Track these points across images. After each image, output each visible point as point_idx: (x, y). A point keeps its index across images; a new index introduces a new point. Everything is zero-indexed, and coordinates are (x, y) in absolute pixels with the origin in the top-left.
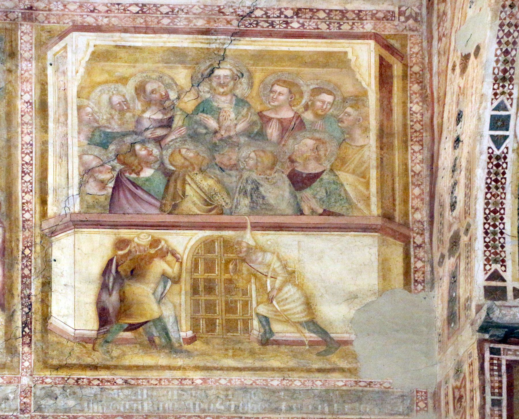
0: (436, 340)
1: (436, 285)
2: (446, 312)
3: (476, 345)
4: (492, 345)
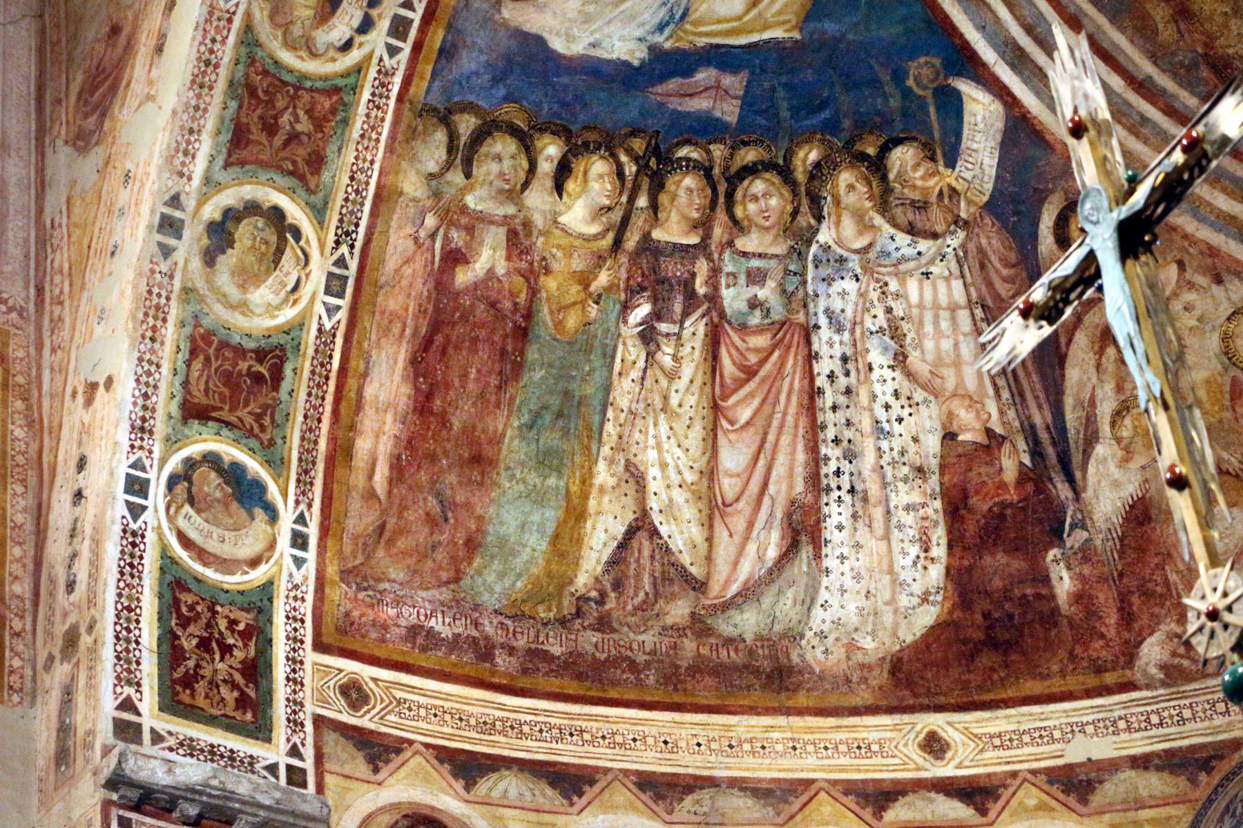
0: (36, 787)
1: (39, 700)
2: (53, 746)
3: (98, 808)
4: (121, 812)
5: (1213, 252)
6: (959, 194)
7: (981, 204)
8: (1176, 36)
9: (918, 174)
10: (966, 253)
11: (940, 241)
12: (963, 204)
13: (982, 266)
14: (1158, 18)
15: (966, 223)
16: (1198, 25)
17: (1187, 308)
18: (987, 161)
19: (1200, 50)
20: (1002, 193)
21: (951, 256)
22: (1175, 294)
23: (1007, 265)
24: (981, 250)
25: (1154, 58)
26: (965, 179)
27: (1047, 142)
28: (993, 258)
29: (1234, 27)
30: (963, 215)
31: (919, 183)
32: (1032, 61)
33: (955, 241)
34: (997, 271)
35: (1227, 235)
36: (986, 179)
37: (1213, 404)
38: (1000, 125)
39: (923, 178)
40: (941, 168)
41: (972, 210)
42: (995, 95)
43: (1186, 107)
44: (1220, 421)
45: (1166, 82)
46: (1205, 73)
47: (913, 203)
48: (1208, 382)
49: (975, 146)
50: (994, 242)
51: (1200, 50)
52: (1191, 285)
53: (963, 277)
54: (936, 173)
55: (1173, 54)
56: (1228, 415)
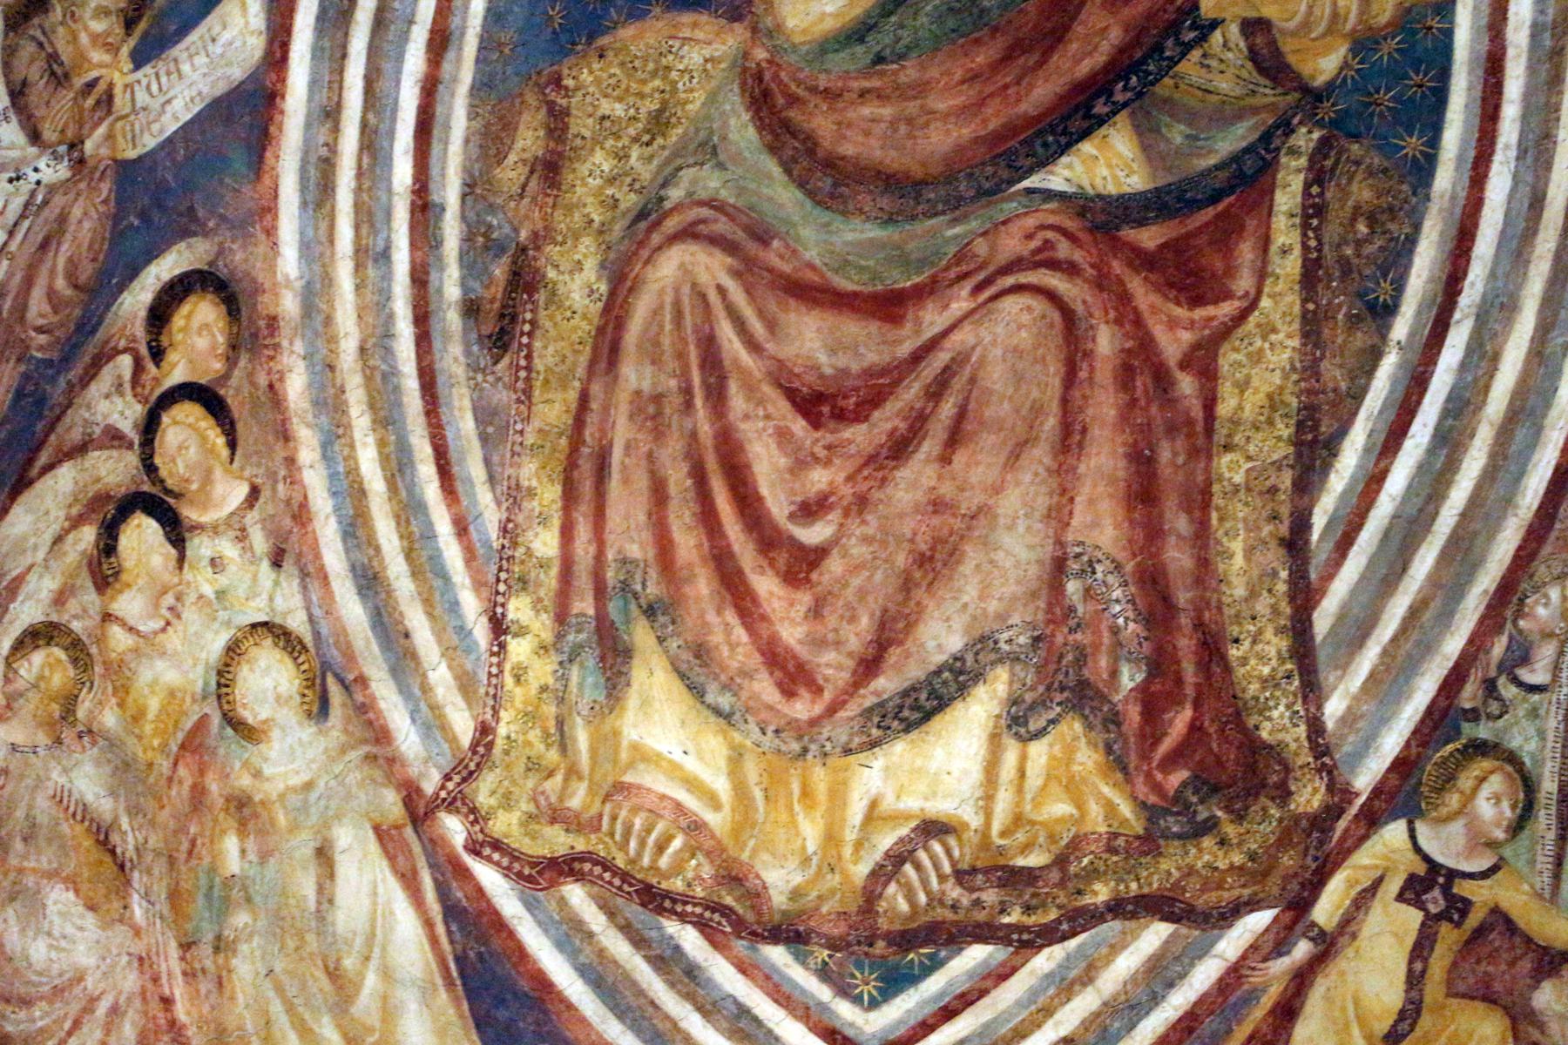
5: (301, 514)
6: (109, 112)
7: (119, 157)
8: (516, 189)
9: (98, 26)
10: (46, 202)
11: (33, 150)
12: (101, 130)
13: (44, 246)
14: (519, 144)
15: (81, 161)
16: (550, 201)
17: (216, 563)
18: (178, 104)
19: (523, 235)
20: (152, 170)
21: (25, 187)
22: (215, 530)
23: (71, 276)
24: (62, 219)
25: (469, 189)
26: (133, 100)
27: (261, 158)
28: (65, 247)
29: (582, 248)
30: (89, 146)
31: (84, 39)
32: (346, 34)
33: (51, 171)
34: (53, 272)
35: (337, 509)
36: (155, 127)
37: (156, 732)
38: (237, 74)
39: (95, 38)
40: (125, 51)
41: (104, 151)
42: (268, 28)
43: (440, 291)
44: (150, 765)
45: (451, 231)
46: (499, 271)
47: (54, 57)
48: (172, 693)
49: (186, 68)
50: (87, 225)
51: (523, 235)
52: (242, 536)
53: (11, 234)
54: (113, 49)
55: (492, 208)
56: (165, 765)
